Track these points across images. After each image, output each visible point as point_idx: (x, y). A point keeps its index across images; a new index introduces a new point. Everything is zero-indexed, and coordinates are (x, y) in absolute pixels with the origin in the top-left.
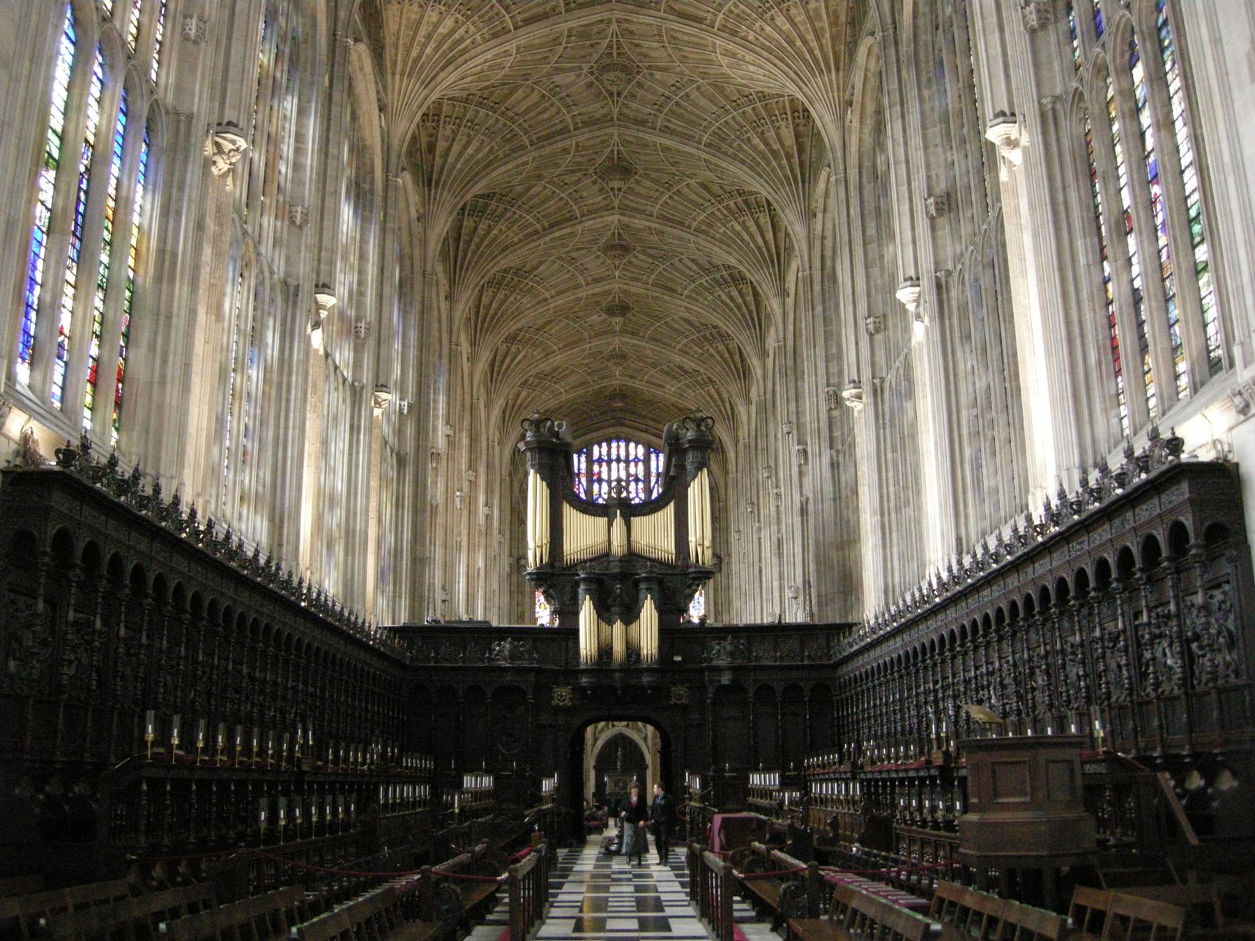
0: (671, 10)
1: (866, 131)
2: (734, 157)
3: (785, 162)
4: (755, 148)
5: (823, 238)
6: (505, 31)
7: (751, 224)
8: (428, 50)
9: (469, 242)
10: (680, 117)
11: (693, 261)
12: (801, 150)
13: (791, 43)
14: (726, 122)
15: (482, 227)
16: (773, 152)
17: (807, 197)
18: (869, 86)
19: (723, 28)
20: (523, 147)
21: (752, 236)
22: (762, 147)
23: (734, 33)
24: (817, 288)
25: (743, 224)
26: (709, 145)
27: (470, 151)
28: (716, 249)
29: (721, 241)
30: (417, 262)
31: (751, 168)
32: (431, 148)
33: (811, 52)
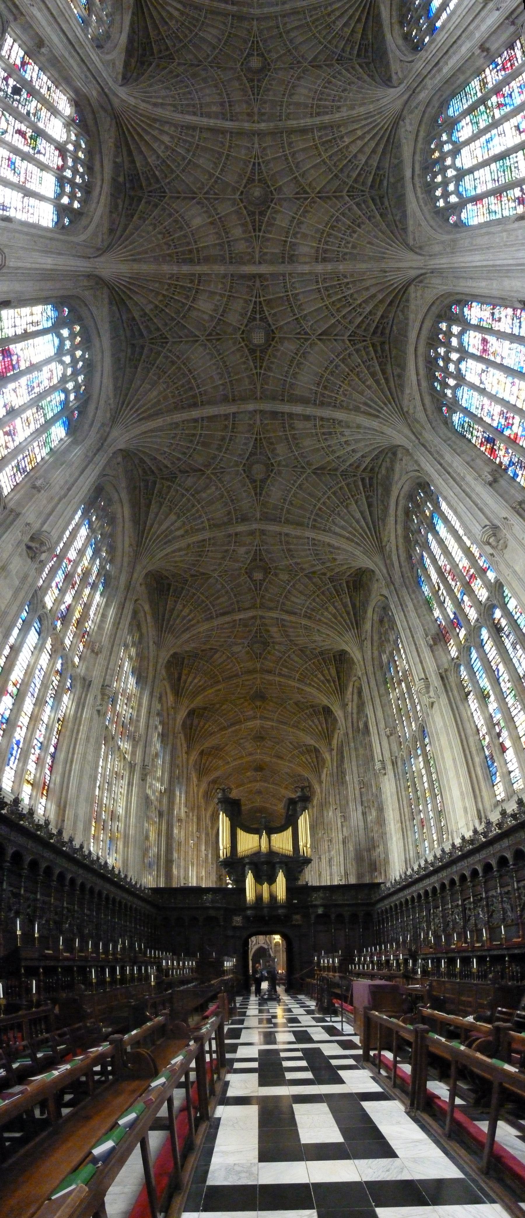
0: (282, 610)
1: (375, 648)
2: (310, 684)
3: (332, 684)
4: (319, 679)
5: (352, 713)
6: (212, 618)
7: (316, 721)
8: (177, 622)
9: (195, 730)
10: (286, 667)
11: (291, 743)
12: (339, 678)
13: (336, 618)
14: (306, 668)
15: (202, 724)
16: (328, 681)
17: (343, 699)
18: (374, 629)
19: (305, 616)
20: (219, 682)
21: (316, 726)
22: (322, 678)
23: (310, 618)
24: (351, 736)
25: (313, 721)
26: (298, 680)
27: (196, 681)
28: (301, 734)
29: (303, 730)
30: (170, 726)
31: (317, 689)
32: (179, 679)
33: (345, 621)
